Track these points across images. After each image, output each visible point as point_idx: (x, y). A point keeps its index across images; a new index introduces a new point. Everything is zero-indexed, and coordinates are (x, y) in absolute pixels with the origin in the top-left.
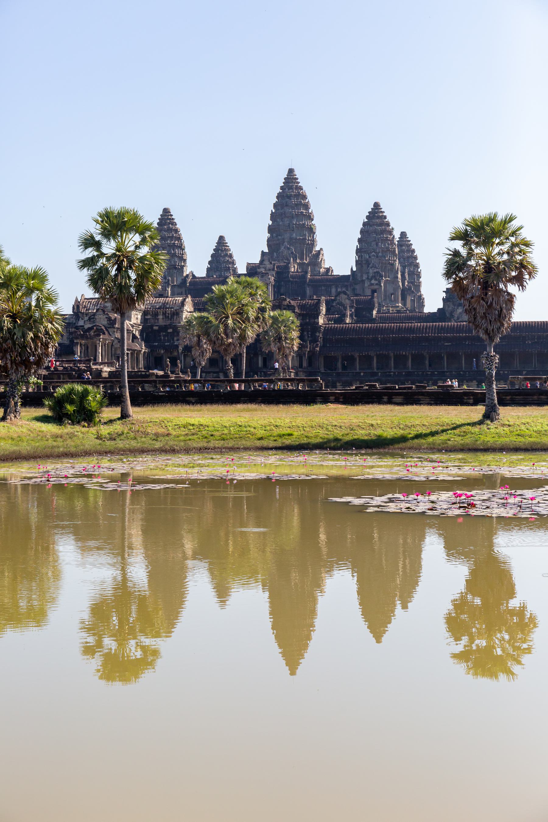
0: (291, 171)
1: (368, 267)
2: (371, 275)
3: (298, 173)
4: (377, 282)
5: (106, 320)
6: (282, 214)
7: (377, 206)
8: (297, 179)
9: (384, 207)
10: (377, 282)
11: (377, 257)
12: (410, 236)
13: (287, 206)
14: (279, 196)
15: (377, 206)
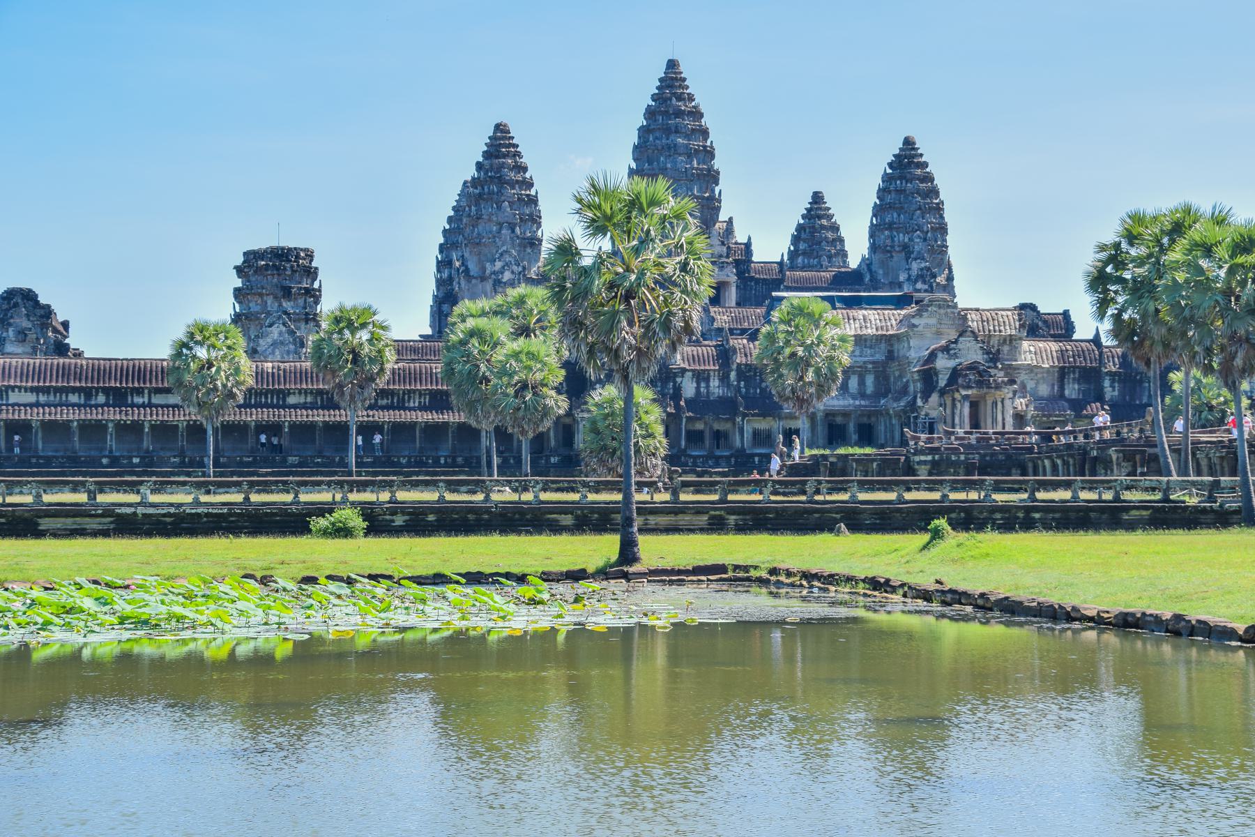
0: (672, 65)
1: (907, 259)
2: (914, 272)
3: (685, 70)
4: (926, 287)
5: (980, 352)
6: (669, 148)
7: (909, 143)
8: (684, 80)
9: (922, 146)
10: (926, 287)
11: (925, 240)
12: (829, 201)
13: (677, 132)
14: (650, 113)
15: (909, 143)
